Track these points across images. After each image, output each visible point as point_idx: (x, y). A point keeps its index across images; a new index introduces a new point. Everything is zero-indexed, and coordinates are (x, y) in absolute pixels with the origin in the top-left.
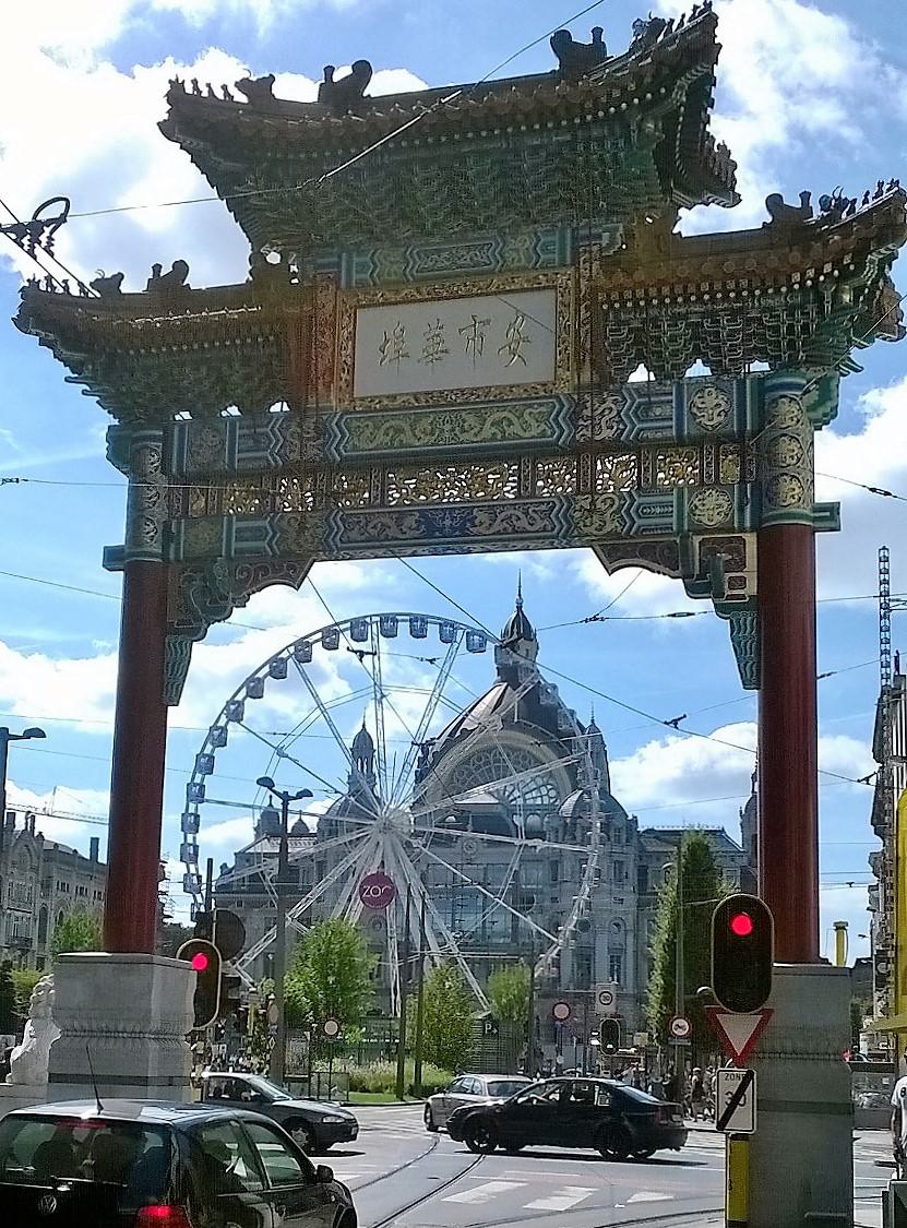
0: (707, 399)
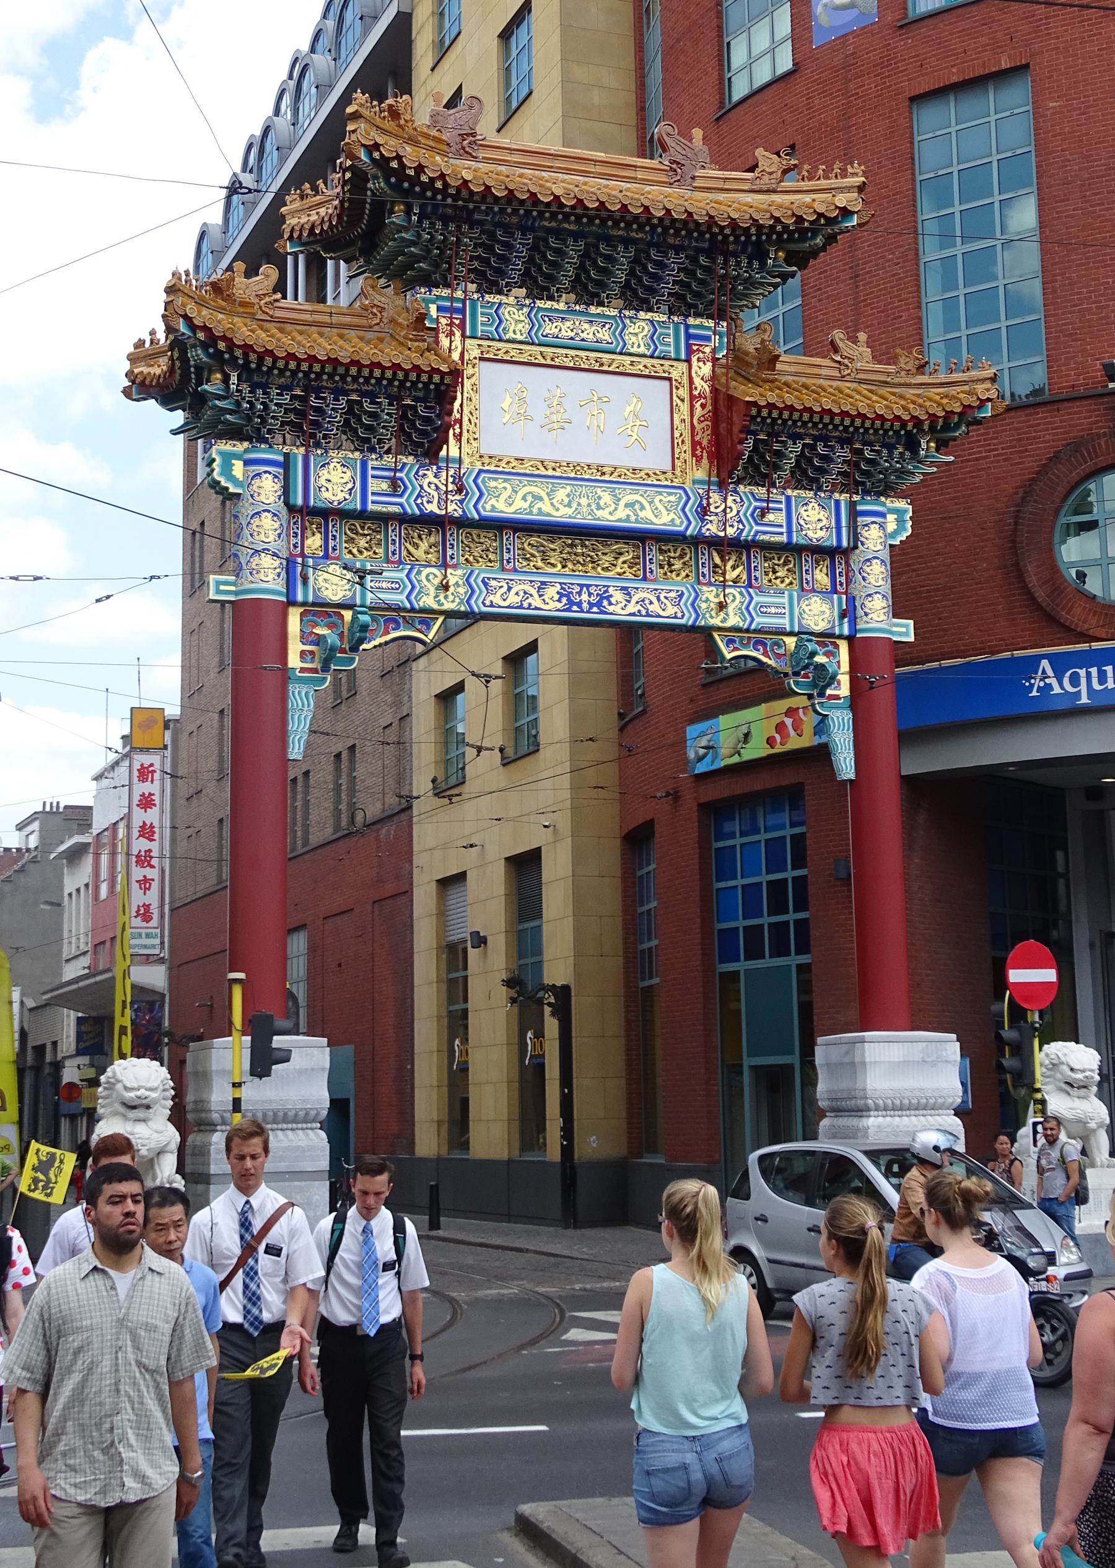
0: (810, 512)
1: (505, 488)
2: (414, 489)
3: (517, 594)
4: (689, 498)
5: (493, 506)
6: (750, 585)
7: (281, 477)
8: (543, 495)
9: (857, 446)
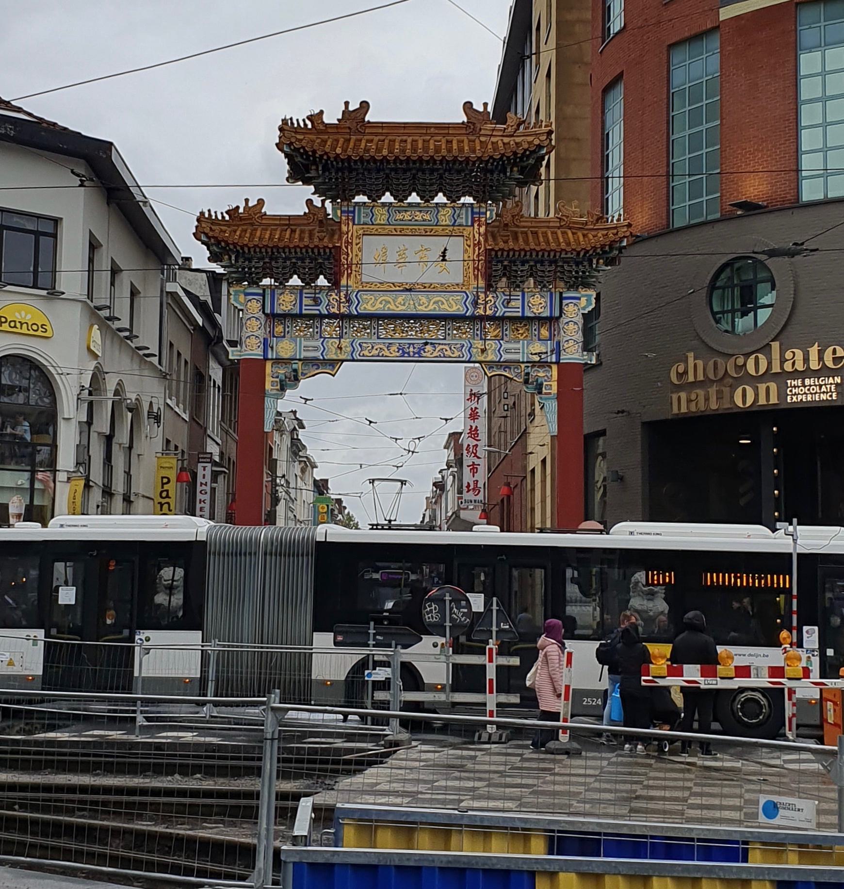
2: (325, 302)
4: (468, 297)
5: (365, 308)
6: (502, 339)
8: (391, 301)
9: (560, 264)
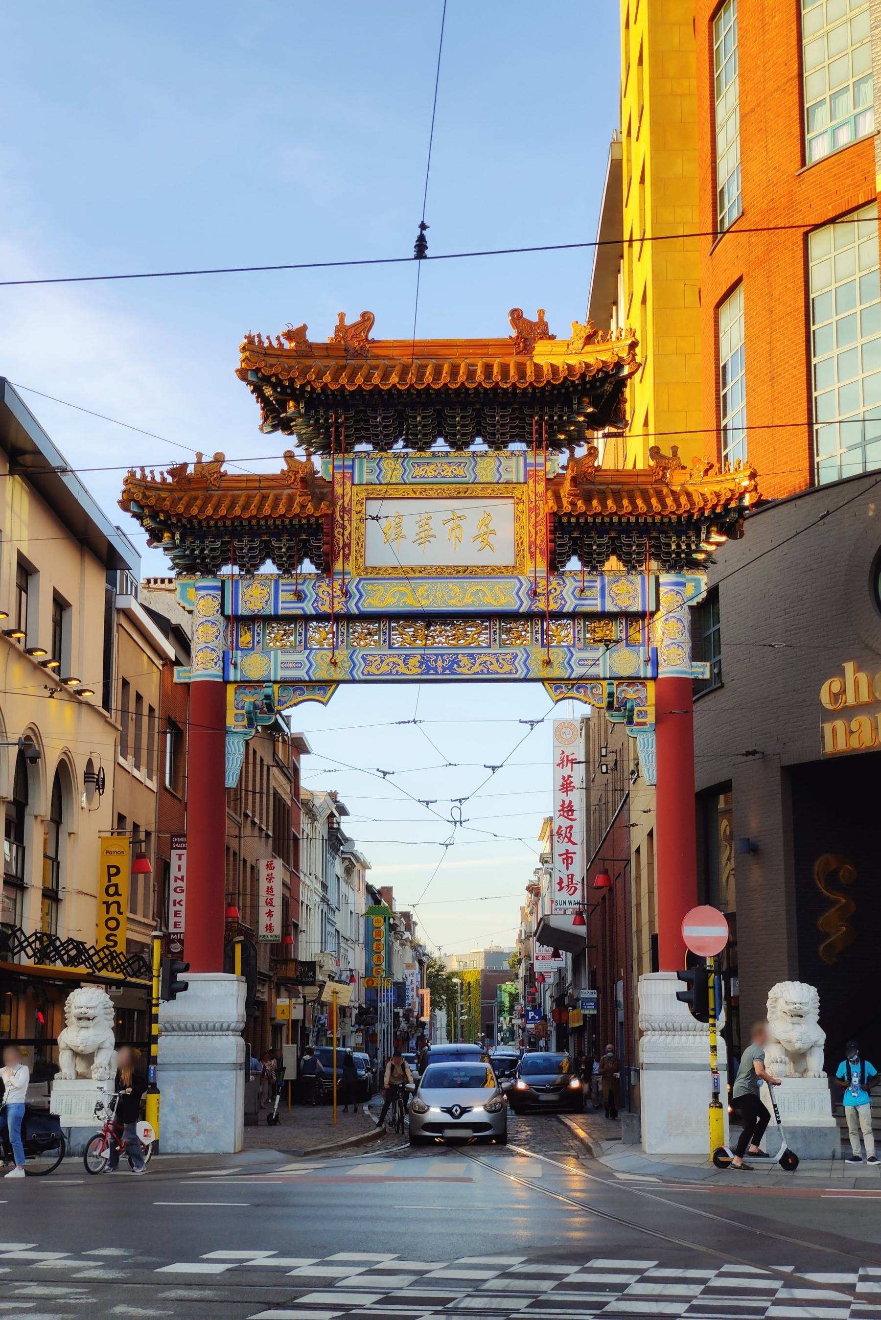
0: (620, 587)
1: (379, 590)
3: (388, 664)
4: (522, 585)
6: (574, 645)
7: (219, 597)
9: (654, 535)
